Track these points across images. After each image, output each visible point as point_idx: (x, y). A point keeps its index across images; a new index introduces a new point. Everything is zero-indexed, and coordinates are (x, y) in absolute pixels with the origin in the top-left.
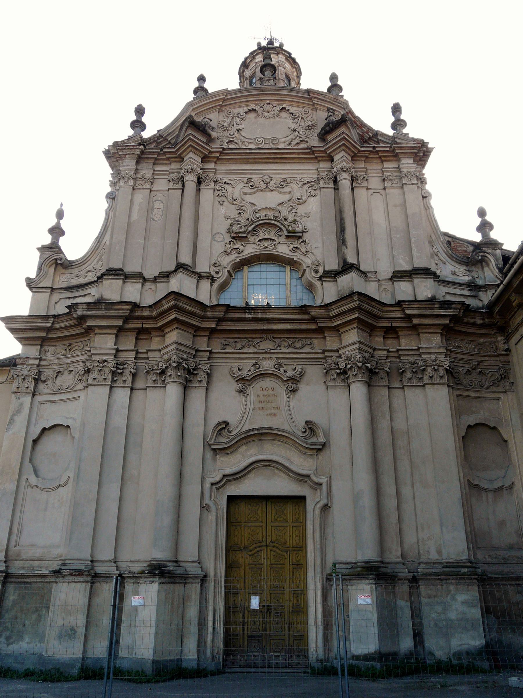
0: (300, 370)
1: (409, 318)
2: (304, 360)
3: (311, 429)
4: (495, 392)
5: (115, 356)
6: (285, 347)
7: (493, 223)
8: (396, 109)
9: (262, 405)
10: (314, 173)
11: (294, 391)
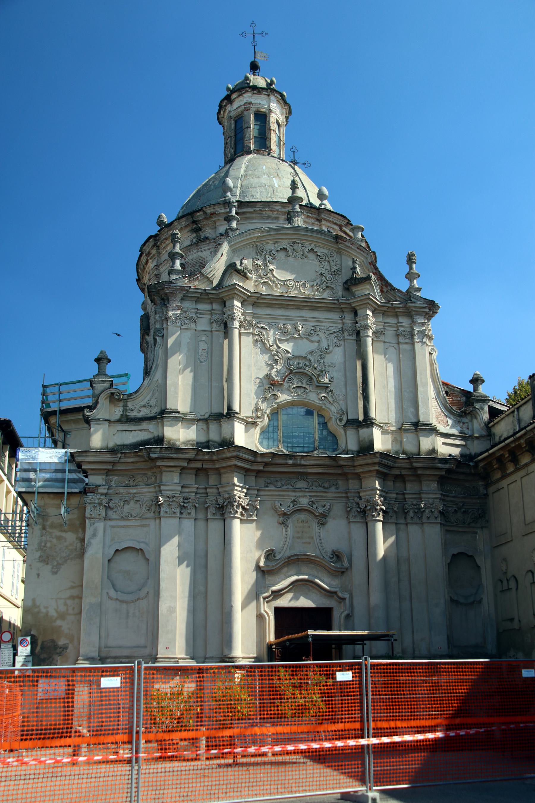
1: (415, 469)
3: (338, 556)
5: (181, 492)
7: (484, 378)
8: (410, 260)
10: (339, 323)
11: (323, 524)
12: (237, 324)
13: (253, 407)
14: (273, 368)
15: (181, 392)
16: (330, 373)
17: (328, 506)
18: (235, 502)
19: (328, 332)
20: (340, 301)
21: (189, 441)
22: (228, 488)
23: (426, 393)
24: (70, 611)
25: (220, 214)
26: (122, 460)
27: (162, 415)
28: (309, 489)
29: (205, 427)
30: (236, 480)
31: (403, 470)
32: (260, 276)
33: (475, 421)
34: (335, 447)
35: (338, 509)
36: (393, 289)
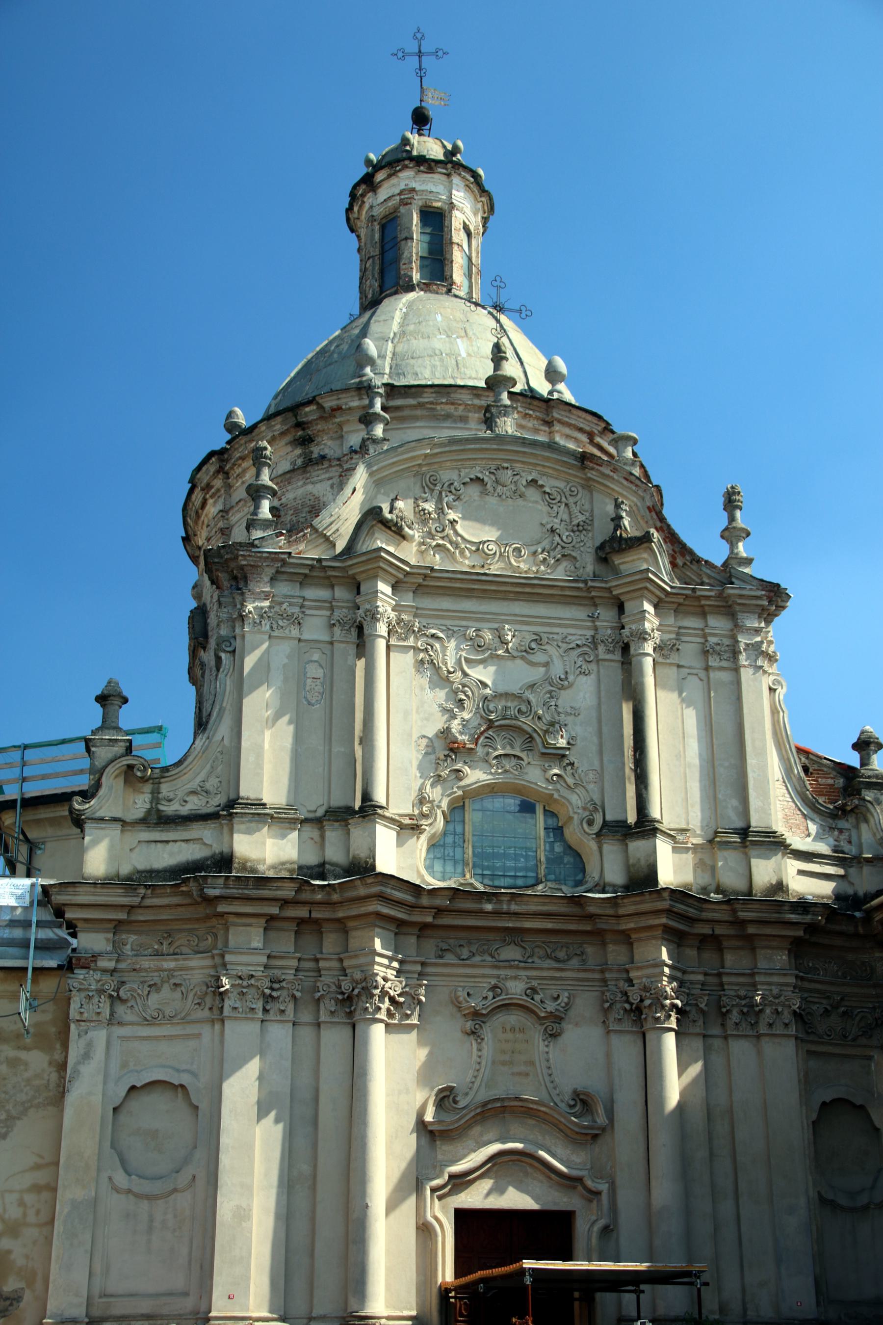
0: (566, 1000)
1: (743, 923)
2: (571, 983)
3: (584, 1102)
4: (865, 1046)
5: (266, 967)
6: (540, 958)
8: (731, 502)
9: (507, 1057)
10: (588, 628)
11: (554, 1036)
12: (382, 629)
13: (414, 794)
14: (454, 717)
15: (268, 763)
16: (569, 726)
17: (564, 998)
18: (376, 987)
19: (564, 646)
20: (590, 584)
21: (283, 864)
22: (362, 960)
23: (763, 768)
24: (32, 1218)
25: (350, 409)
26: (148, 902)
27: (231, 810)
28: (526, 963)
29: (316, 834)
30: (378, 944)
31: (719, 927)
32: (430, 533)
33: (864, 827)
34: (580, 877)
35: (585, 1004)
36: (696, 560)
